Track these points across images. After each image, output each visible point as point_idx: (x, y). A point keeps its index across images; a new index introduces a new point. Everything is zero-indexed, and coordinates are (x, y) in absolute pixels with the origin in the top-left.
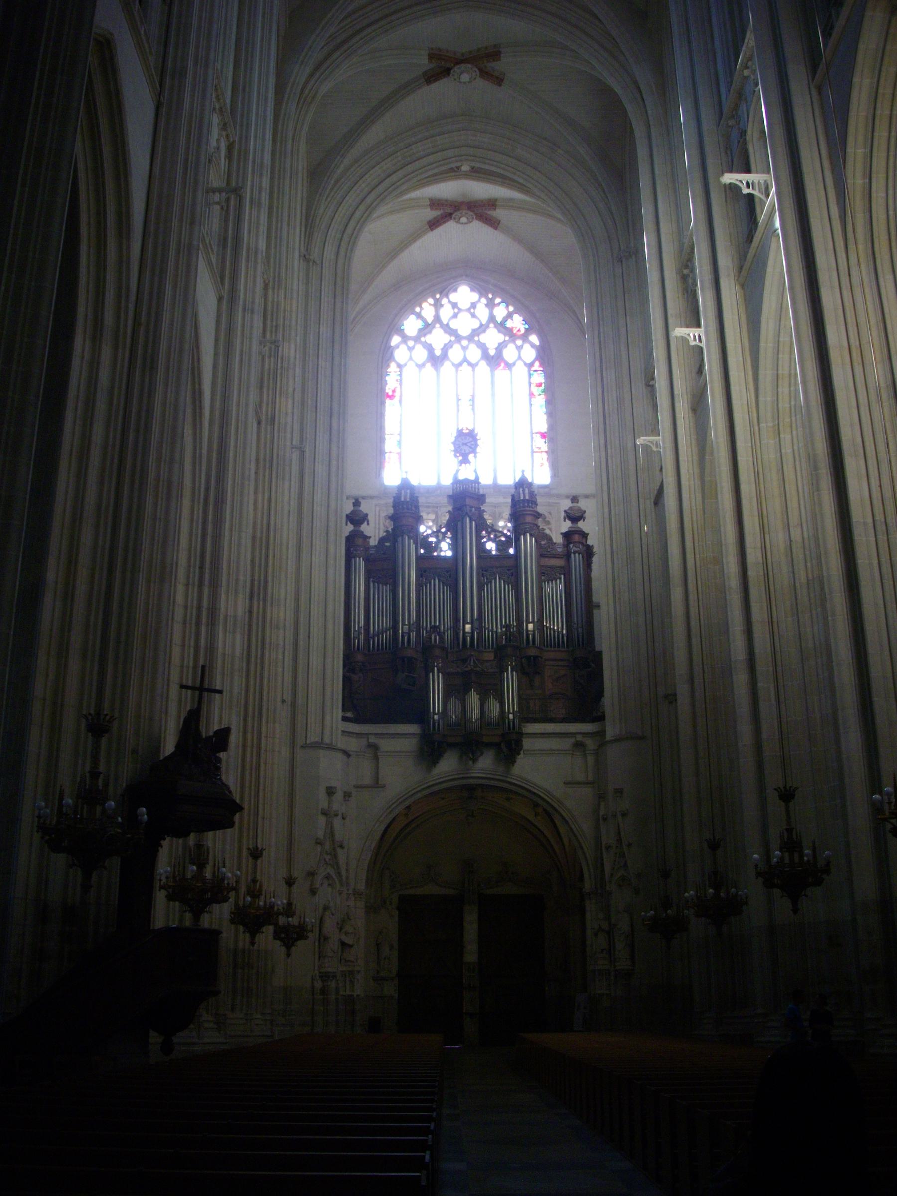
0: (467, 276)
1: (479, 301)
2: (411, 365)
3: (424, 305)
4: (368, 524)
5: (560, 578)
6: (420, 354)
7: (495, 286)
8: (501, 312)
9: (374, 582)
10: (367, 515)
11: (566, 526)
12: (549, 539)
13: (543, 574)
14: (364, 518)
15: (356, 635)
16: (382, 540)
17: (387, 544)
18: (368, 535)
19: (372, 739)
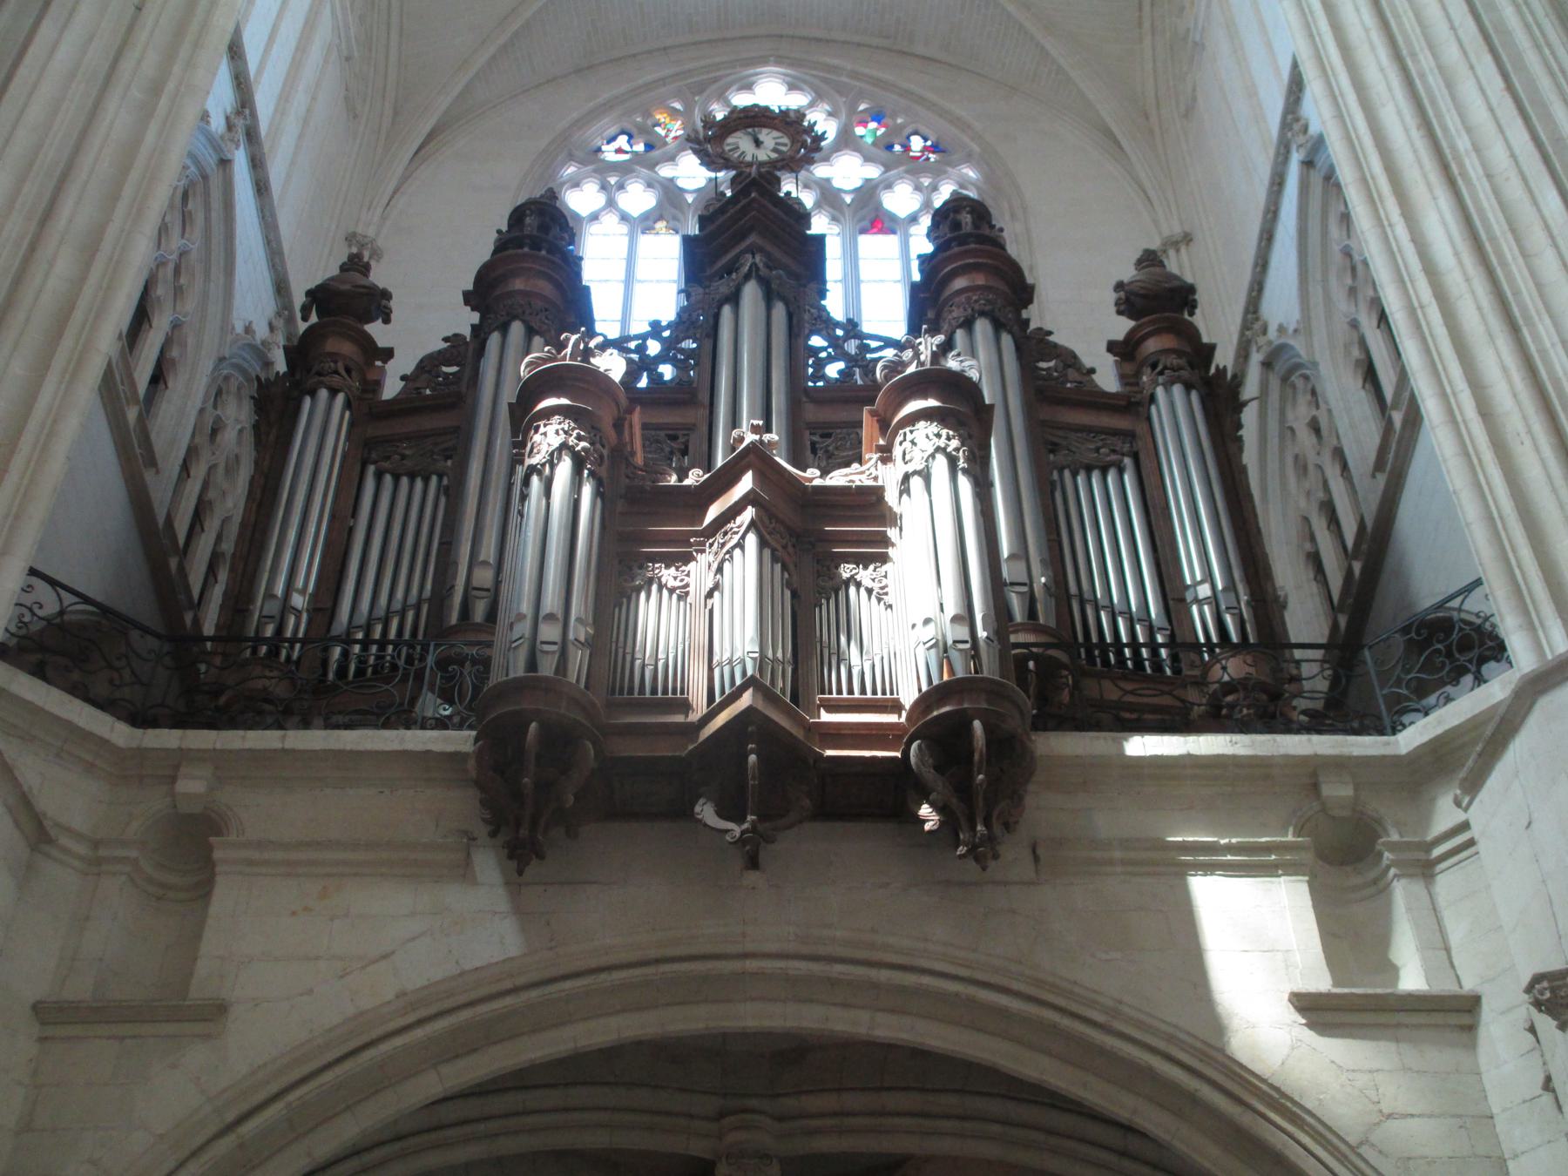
0: (780, 61)
1: (811, 105)
2: (610, 220)
3: (661, 117)
4: (387, 321)
5: (1121, 471)
6: (638, 198)
7: (855, 75)
8: (868, 132)
9: (379, 477)
10: (386, 295)
11: (1122, 327)
12: (1069, 359)
13: (1054, 448)
14: (377, 304)
15: (273, 608)
16: (429, 365)
17: (445, 369)
18: (381, 343)
19: (192, 785)
